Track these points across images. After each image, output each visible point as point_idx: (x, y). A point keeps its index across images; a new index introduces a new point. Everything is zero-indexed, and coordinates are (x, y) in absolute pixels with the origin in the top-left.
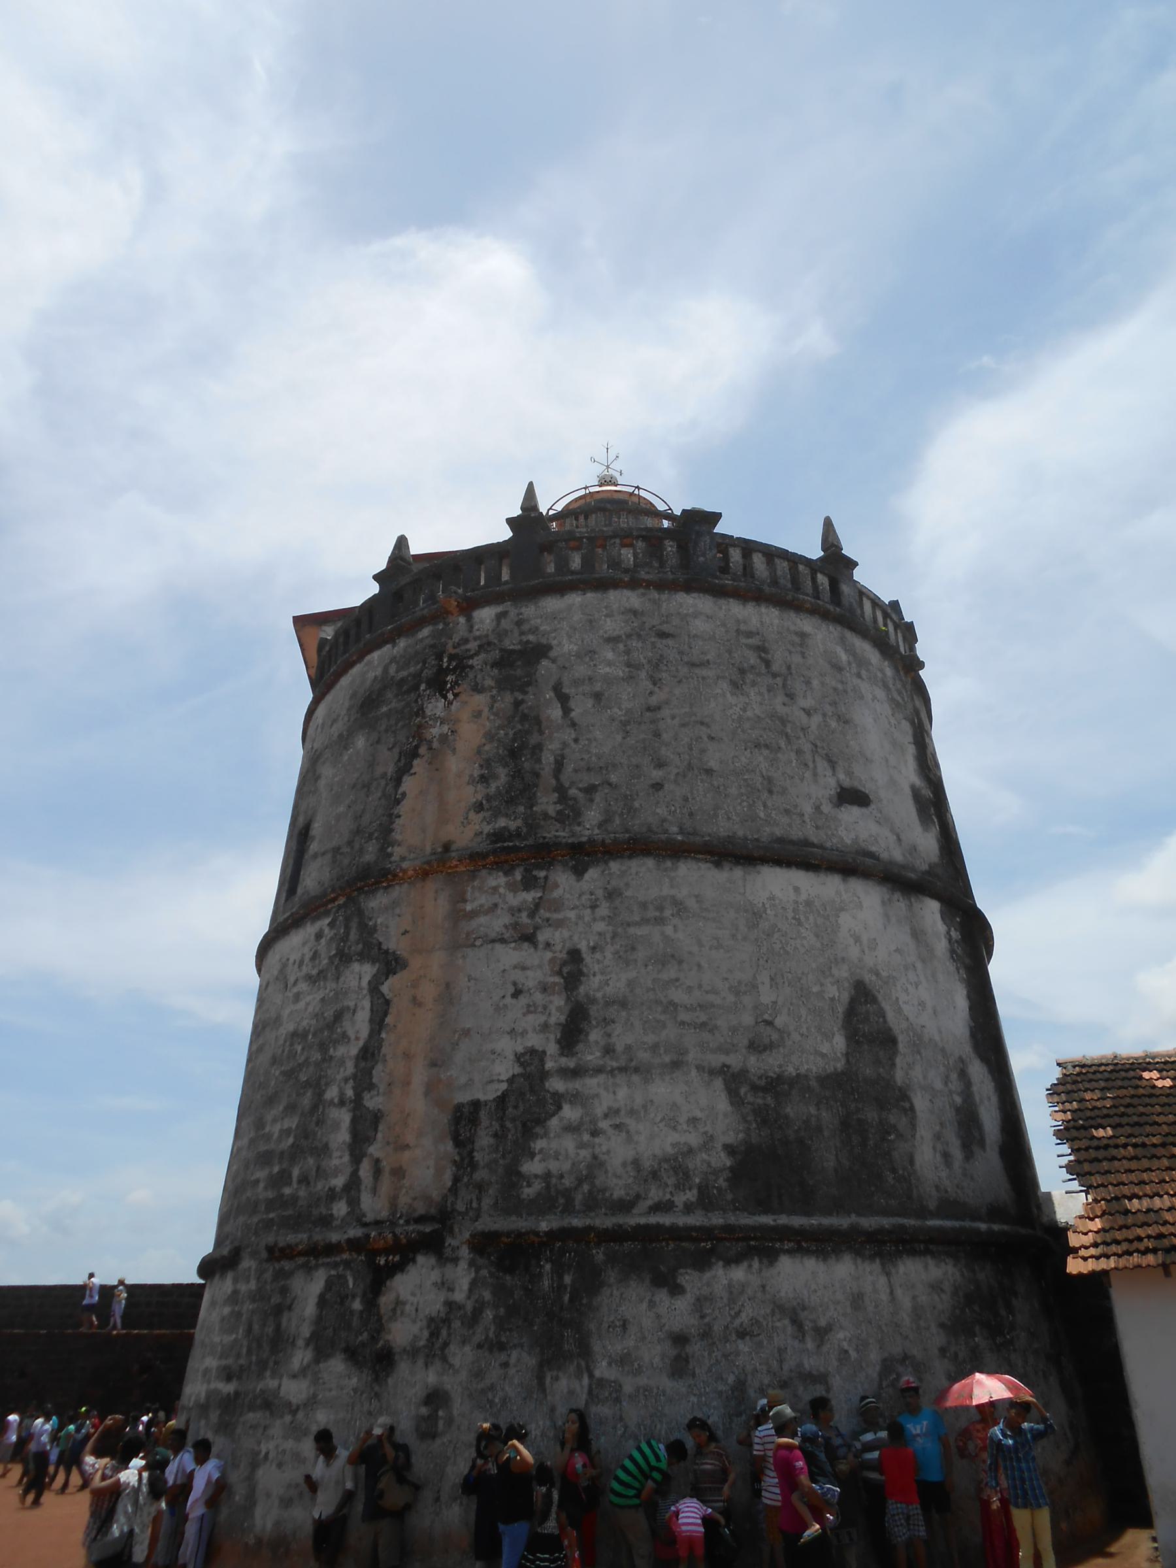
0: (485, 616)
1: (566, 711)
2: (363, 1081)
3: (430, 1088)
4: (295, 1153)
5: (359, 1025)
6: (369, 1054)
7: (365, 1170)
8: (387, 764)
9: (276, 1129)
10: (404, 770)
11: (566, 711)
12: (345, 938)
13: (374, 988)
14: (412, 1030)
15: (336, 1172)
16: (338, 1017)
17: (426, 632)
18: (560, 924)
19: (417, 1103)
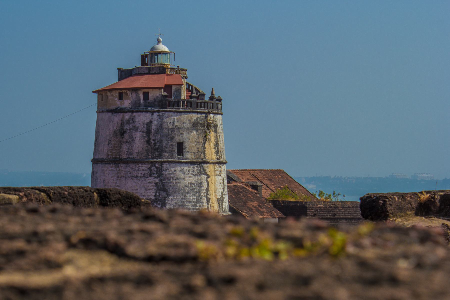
0: (212, 115)
2: (207, 194)
3: (215, 195)
4: (197, 202)
5: (205, 184)
6: (207, 189)
7: (209, 206)
8: (202, 140)
9: (191, 198)
10: (205, 143)
12: (200, 170)
13: (207, 179)
14: (212, 187)
15: (205, 206)
16: (201, 183)
19: (214, 198)
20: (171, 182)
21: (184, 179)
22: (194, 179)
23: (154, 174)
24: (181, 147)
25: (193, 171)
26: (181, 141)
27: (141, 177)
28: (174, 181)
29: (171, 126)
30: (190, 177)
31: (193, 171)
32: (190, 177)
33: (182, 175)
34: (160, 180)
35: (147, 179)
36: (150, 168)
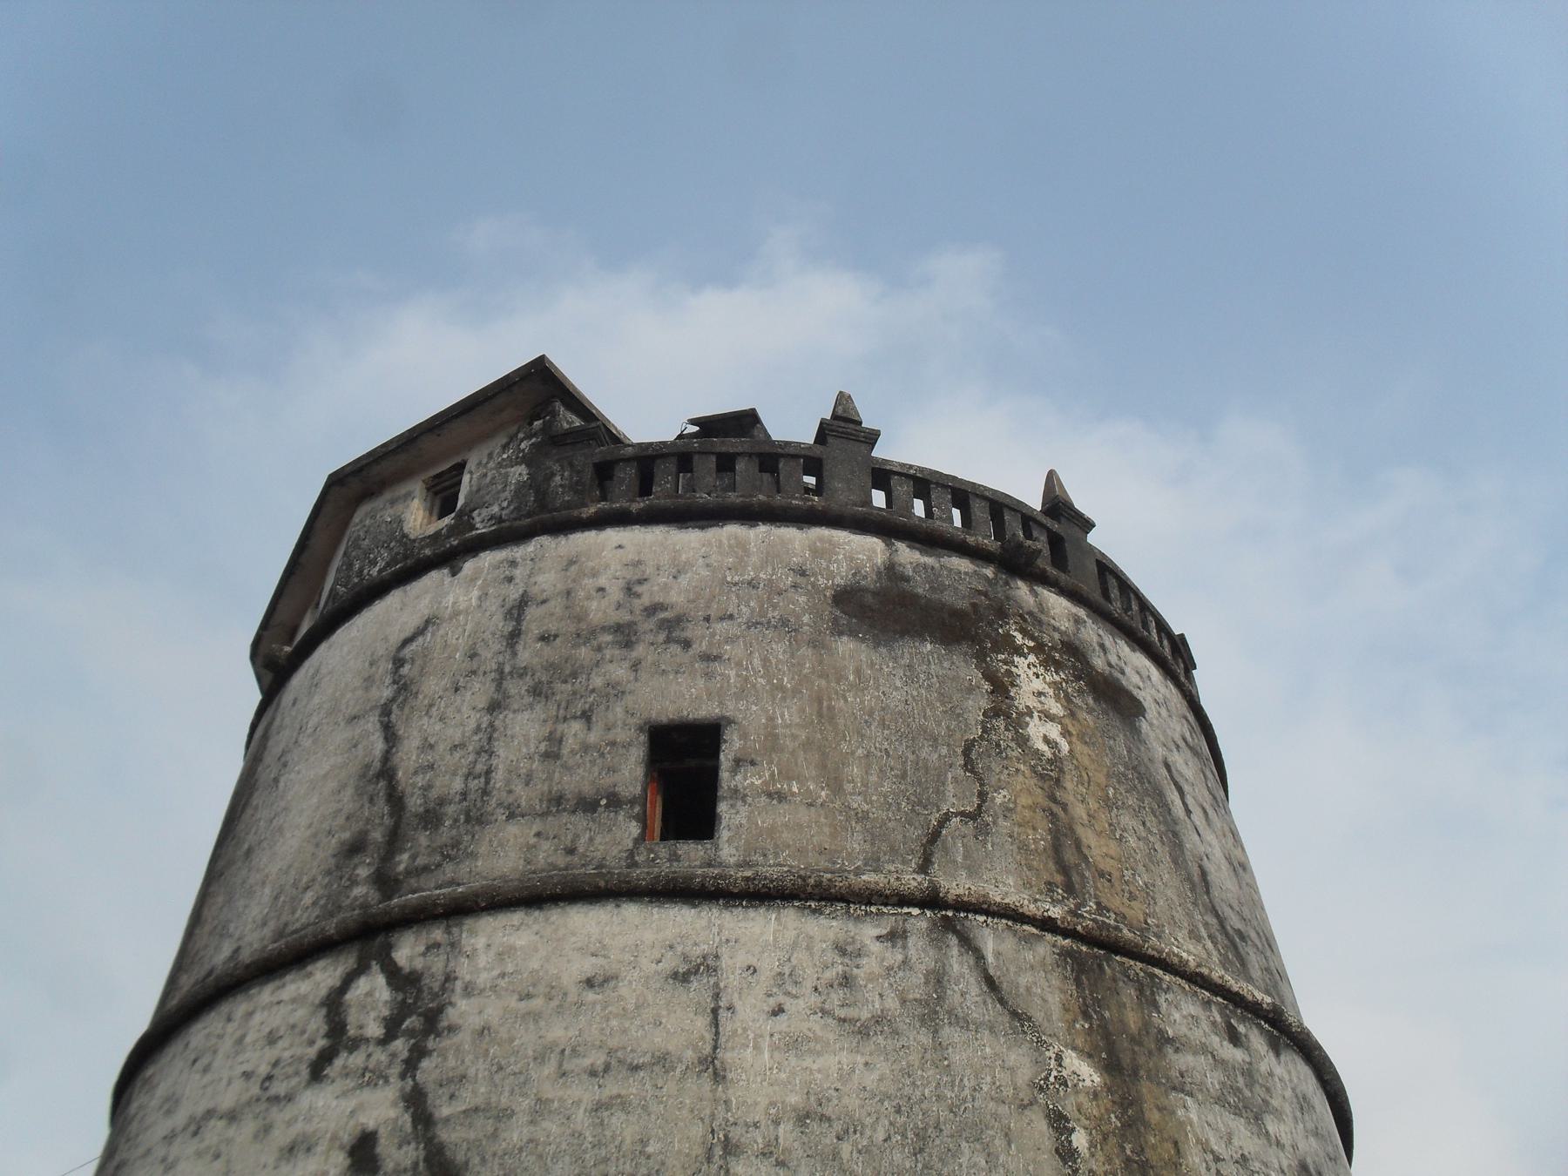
1: (1188, 812)
11: (1188, 812)
12: (938, 979)
17: (962, 564)
18: (1278, 1114)
20: (541, 1107)
21: (712, 1066)
22: (847, 1072)
23: (355, 1044)
24: (685, 772)
25: (846, 981)
26: (706, 711)
27: (232, 1116)
28: (583, 1093)
29: (600, 611)
30: (794, 1044)
31: (846, 981)
32: (794, 1044)
33: (679, 1026)
34: (416, 1101)
35: (279, 1116)
36: (334, 1004)
